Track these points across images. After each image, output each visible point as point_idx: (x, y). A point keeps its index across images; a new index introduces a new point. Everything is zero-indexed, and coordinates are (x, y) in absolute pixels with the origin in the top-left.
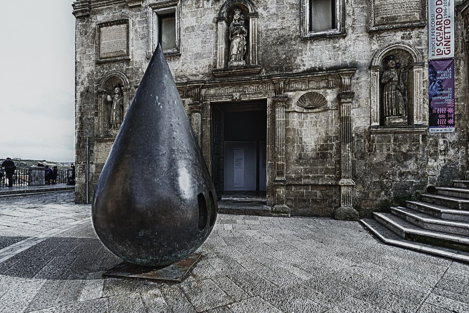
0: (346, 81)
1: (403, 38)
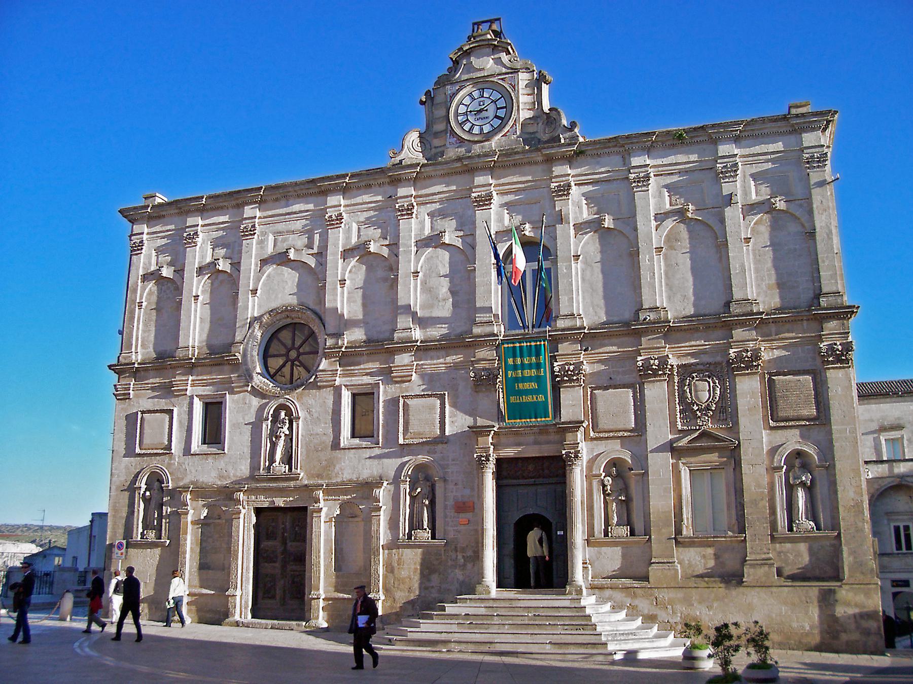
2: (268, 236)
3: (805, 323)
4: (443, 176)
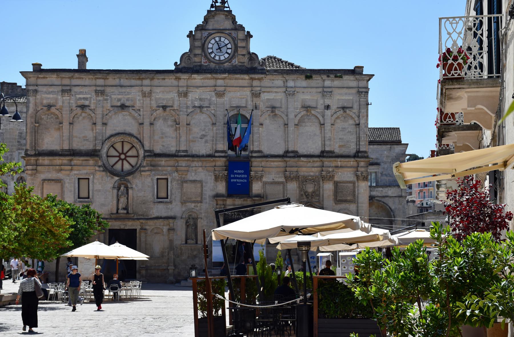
0: (171, 225)
1: (194, 207)
2: (111, 97)
3: (352, 162)
4: (201, 79)
